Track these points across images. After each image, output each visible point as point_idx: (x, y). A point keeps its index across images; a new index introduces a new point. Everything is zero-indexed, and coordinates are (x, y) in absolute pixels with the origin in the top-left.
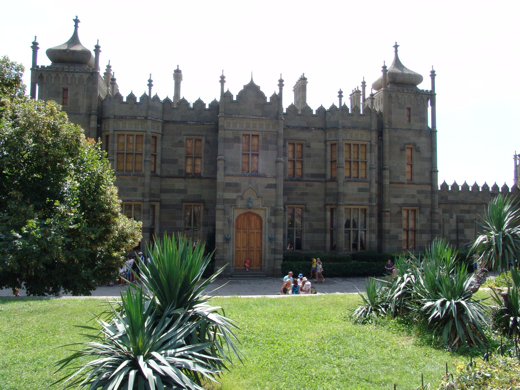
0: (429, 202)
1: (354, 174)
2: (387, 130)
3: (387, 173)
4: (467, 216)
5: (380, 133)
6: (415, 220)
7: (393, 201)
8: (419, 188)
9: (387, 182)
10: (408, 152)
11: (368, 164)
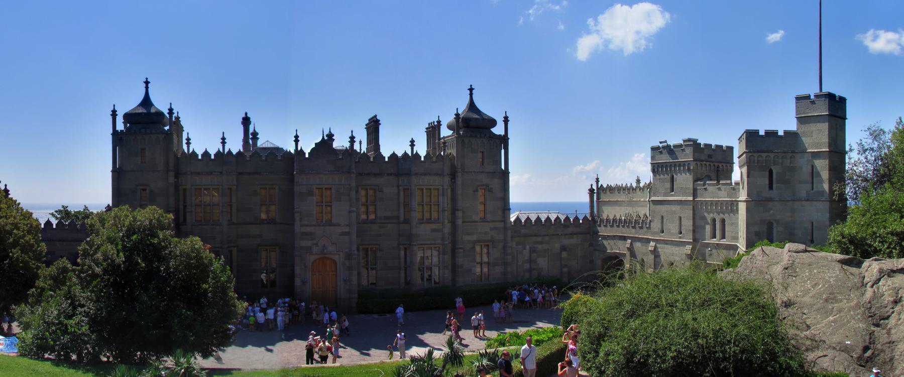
0: (501, 237)
1: (427, 215)
2: (460, 174)
3: (459, 214)
4: (540, 247)
5: (453, 176)
6: (488, 253)
7: (467, 238)
8: (491, 225)
9: (459, 222)
10: (480, 192)
11: (441, 206)
